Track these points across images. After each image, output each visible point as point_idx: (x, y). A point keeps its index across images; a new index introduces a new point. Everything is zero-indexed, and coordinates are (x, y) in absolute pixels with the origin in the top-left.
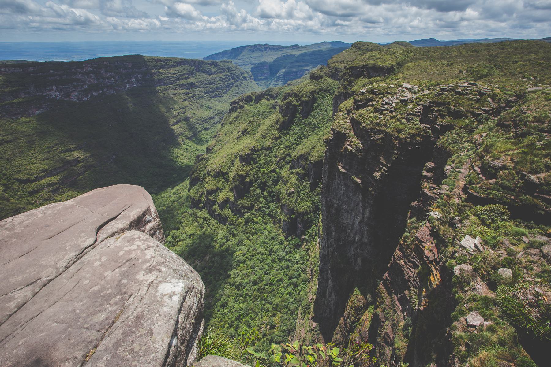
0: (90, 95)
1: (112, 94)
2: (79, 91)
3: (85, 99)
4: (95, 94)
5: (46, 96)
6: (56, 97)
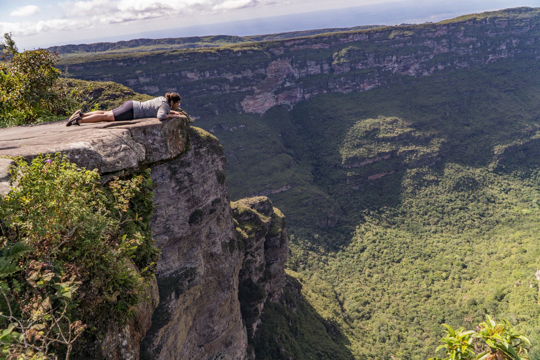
0: (433, 69)
1: (464, 68)
2: (421, 63)
3: (426, 74)
4: (440, 67)
5: (382, 68)
6: (393, 69)
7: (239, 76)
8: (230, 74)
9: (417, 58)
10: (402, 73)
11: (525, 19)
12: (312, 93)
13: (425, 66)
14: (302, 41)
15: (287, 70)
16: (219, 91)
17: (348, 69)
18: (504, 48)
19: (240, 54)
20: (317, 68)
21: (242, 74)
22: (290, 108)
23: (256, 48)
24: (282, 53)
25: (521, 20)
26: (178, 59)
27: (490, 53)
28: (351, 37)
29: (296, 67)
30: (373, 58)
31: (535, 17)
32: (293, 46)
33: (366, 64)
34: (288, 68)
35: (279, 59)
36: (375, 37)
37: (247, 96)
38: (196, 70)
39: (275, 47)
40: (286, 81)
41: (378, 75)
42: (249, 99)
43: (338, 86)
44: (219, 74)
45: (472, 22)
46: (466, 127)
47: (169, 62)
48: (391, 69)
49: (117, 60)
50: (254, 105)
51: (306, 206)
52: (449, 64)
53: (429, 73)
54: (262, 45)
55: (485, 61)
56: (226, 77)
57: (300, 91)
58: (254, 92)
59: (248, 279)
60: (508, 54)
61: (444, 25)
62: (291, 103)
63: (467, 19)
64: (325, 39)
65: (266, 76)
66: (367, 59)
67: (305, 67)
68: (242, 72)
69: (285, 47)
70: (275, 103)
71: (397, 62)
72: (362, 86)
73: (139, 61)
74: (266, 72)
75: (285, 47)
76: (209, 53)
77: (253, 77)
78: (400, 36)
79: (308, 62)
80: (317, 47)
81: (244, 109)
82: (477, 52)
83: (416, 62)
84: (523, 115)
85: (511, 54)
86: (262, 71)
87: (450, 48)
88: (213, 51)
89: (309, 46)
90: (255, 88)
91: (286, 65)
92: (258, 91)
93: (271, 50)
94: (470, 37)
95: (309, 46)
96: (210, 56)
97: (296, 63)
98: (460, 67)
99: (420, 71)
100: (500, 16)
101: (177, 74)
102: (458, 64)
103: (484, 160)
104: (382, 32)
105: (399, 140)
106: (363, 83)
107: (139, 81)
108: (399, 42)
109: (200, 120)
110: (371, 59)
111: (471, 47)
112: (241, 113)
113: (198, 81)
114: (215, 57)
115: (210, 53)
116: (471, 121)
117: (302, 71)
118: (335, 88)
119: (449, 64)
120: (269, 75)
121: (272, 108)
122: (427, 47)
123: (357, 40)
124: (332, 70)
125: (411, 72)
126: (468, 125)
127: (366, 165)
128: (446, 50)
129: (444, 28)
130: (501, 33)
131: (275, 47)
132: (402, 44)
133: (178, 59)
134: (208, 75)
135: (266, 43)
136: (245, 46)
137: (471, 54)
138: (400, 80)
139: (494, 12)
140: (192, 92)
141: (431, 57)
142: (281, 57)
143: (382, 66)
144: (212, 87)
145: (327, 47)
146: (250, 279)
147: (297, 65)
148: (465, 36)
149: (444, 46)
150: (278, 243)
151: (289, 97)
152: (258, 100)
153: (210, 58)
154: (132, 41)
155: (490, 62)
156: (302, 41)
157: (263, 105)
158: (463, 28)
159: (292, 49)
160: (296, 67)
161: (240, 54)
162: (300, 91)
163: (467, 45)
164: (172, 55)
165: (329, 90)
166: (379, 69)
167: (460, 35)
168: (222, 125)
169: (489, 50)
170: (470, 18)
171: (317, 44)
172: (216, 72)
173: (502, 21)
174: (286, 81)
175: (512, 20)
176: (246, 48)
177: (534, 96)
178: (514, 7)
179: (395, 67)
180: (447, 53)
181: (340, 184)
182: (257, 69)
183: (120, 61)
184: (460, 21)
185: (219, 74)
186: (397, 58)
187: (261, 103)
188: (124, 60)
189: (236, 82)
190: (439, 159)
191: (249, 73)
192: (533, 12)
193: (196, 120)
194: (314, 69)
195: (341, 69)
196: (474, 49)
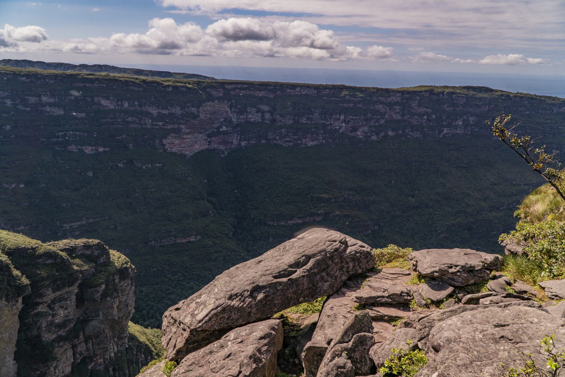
0: (382, 134)
1: (416, 138)
2: (370, 126)
3: (374, 138)
4: (390, 133)
5: (328, 125)
6: (340, 129)
7: (165, 112)
8: (154, 108)
9: (366, 120)
10: (350, 134)
11: (484, 98)
12: (249, 142)
13: (374, 130)
14: (245, 86)
15: (225, 114)
16: (137, 124)
17: (291, 122)
18: (461, 123)
19: (171, 89)
20: (257, 116)
21: (169, 110)
22: (223, 152)
23: (191, 86)
24: (221, 95)
25: (480, 99)
26: (93, 84)
27: (445, 126)
28: (298, 89)
29: (235, 112)
30: (320, 114)
31: (495, 98)
32: (234, 89)
33: (311, 119)
34: (227, 112)
35: (217, 101)
36: (324, 92)
37: (172, 135)
38: (112, 98)
39: (213, 87)
40: (222, 124)
41: (322, 132)
42: (175, 137)
43: (278, 138)
44: (140, 106)
45: (428, 93)
46: (411, 198)
47: (82, 85)
48: (338, 127)
49: (19, 75)
50: (180, 145)
51: (215, 260)
52: (401, 132)
53: (378, 138)
54: (198, 83)
55: (439, 134)
56: (149, 110)
57: (237, 137)
58: (181, 131)
59: (36, 336)
60: (465, 130)
61: (398, 91)
62: (226, 149)
63: (423, 89)
64: (271, 88)
65: (198, 116)
66: (313, 114)
67: (245, 114)
68: (169, 108)
69: (224, 89)
70: (207, 147)
71: (344, 121)
72: (304, 141)
73: (45, 79)
74: (198, 112)
75: (224, 89)
76: (131, 82)
77: (182, 114)
78: (350, 96)
79: (249, 108)
80: (261, 94)
81: (166, 147)
82: (431, 124)
83: (366, 125)
84: (471, 194)
85: (468, 131)
86: (194, 110)
87: (403, 115)
88: (137, 81)
89: (252, 93)
90: (182, 126)
91: (224, 108)
92: (187, 131)
93: (208, 90)
94: (425, 107)
95: (252, 93)
96: (133, 86)
97: (236, 107)
98: (412, 136)
99: (369, 134)
100: (458, 91)
101: (89, 99)
102: (410, 133)
103: (425, 235)
104: (332, 89)
105: (335, 202)
106: (306, 138)
107: (41, 101)
108: (349, 102)
109: (108, 151)
110: (317, 115)
111: (425, 117)
112: (161, 151)
113: (113, 110)
114: (138, 87)
115: (134, 82)
116: (417, 192)
117: (241, 117)
118: (275, 139)
119: (401, 132)
120: (202, 116)
121: (202, 151)
122: (378, 111)
123: (304, 93)
124: (274, 121)
125: (359, 133)
126: (413, 196)
127: (294, 224)
128: (399, 117)
129: (398, 95)
130: (458, 109)
131: (213, 87)
132: (352, 104)
133: (93, 84)
134: (126, 105)
135: (203, 82)
136: (179, 82)
137: (425, 125)
138: (346, 140)
139: (454, 87)
140: (105, 120)
141: (382, 122)
142: (219, 99)
143: (327, 123)
144: (130, 119)
145: (271, 96)
146: (39, 336)
147: (236, 110)
148: (420, 105)
149: (397, 112)
150: (98, 296)
151: (224, 142)
152: (187, 140)
153: (132, 88)
154: (95, 65)
155: (444, 135)
156: (245, 86)
157: (192, 146)
158: (418, 98)
159: (232, 93)
160: (235, 112)
161: (171, 89)
162: (237, 137)
163: (421, 115)
164: (87, 78)
165: (267, 140)
166: (325, 126)
167: (414, 104)
168: (134, 161)
169: (444, 123)
170: (426, 89)
171: (260, 91)
172: (136, 103)
173: (459, 96)
174: (222, 124)
175: (471, 97)
176: (178, 84)
177: (485, 176)
178: (475, 86)
179: (342, 127)
180: (398, 120)
181: (262, 242)
182: (188, 107)
183: (23, 76)
184: (416, 90)
185: (140, 106)
186: (345, 117)
187: (191, 144)
188: (28, 75)
189: (160, 117)
190: (376, 228)
191: (177, 111)
192: (493, 93)
193: (104, 152)
194: (254, 117)
195: (283, 121)
196: (429, 120)
